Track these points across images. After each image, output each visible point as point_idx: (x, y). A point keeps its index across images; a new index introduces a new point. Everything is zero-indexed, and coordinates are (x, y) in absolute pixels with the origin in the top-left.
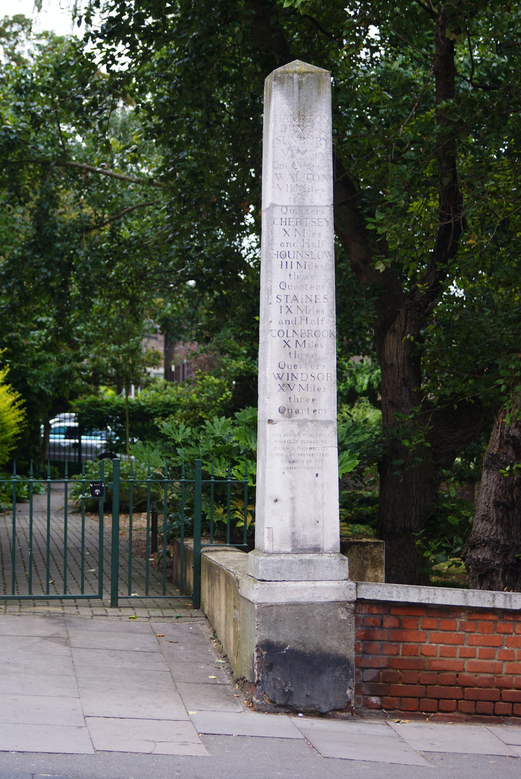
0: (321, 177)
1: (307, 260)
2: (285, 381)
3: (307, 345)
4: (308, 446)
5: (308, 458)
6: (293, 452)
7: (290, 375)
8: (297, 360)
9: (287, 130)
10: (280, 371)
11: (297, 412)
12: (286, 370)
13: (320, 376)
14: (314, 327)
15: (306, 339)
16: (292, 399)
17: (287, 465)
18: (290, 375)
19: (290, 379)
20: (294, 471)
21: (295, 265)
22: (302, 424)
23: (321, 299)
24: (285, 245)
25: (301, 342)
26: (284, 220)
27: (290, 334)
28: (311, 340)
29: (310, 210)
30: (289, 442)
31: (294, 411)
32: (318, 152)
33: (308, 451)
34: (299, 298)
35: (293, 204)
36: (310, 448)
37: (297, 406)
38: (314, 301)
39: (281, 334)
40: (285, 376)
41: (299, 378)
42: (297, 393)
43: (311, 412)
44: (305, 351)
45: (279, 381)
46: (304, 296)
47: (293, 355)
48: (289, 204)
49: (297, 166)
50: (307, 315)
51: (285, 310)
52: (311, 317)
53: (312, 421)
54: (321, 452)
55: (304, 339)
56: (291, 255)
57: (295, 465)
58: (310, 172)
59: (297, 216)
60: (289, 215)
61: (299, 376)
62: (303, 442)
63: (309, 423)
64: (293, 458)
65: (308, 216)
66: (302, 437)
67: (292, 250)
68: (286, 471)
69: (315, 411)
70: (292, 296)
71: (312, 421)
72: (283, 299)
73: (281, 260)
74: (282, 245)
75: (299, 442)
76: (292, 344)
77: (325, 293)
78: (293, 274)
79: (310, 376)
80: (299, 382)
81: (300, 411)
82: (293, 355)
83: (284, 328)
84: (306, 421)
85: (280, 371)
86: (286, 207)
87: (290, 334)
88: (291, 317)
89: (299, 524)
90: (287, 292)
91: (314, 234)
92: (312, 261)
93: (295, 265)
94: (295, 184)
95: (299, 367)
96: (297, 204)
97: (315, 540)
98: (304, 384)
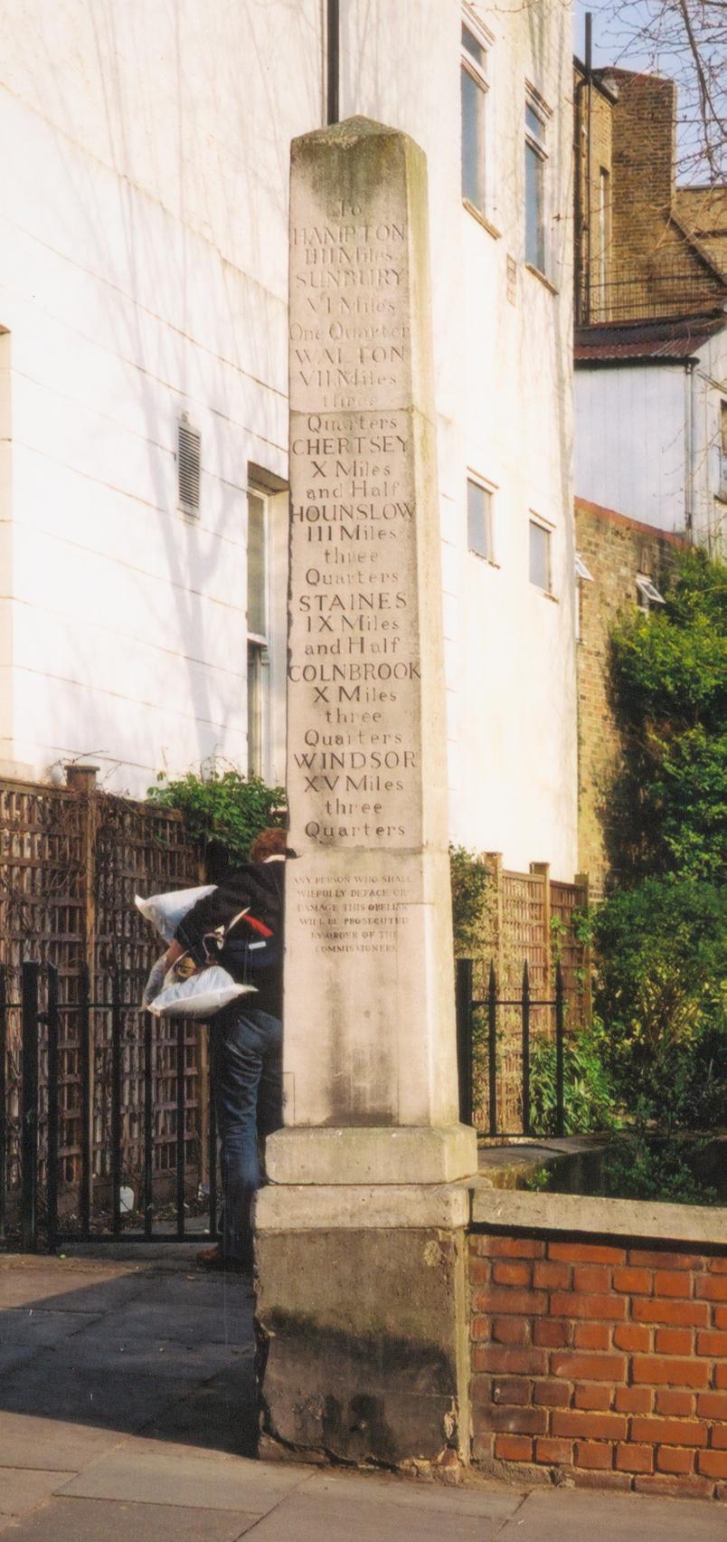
4: (367, 901)
6: (334, 915)
7: (328, 758)
10: (308, 750)
12: (320, 748)
13: (392, 759)
14: (378, 659)
15: (361, 682)
17: (321, 942)
18: (328, 758)
20: (336, 954)
24: (317, 494)
26: (313, 444)
27: (328, 673)
30: (327, 894)
31: (336, 831)
33: (365, 914)
34: (346, 601)
35: (331, 408)
36: (371, 908)
37: (343, 821)
39: (310, 674)
40: (318, 760)
42: (341, 793)
43: (372, 833)
45: (305, 771)
47: (334, 718)
51: (317, 624)
52: (371, 637)
56: (329, 515)
57: (340, 943)
64: (336, 928)
65: (360, 433)
67: (329, 502)
72: (314, 603)
74: (310, 493)
76: (332, 694)
79: (369, 759)
80: (346, 771)
82: (334, 718)
84: (360, 850)
85: (308, 750)
86: (318, 416)
87: (328, 673)
88: (328, 639)
89: (349, 1067)
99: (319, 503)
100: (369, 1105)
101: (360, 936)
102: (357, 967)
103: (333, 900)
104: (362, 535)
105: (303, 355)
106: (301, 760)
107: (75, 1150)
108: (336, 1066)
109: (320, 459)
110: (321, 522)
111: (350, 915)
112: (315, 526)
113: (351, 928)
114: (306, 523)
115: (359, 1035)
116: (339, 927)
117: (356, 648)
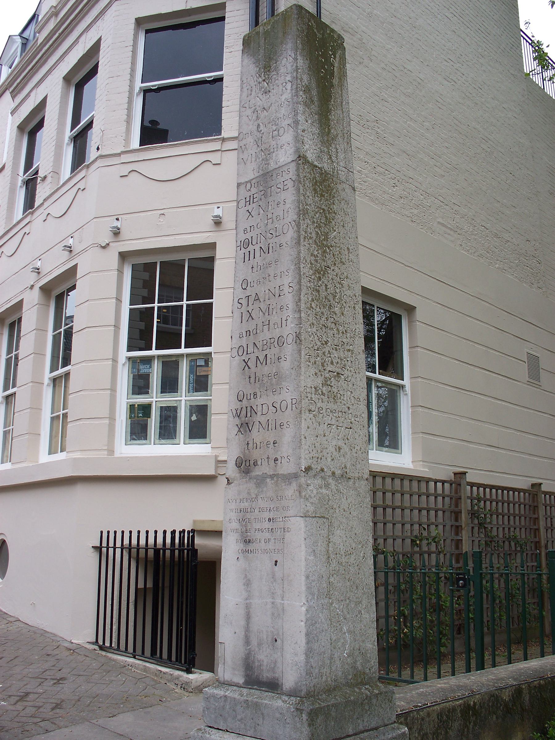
1: (270, 241)
2: (243, 419)
3: (268, 361)
4: (267, 515)
5: (267, 535)
7: (249, 409)
8: (257, 385)
14: (277, 333)
16: (251, 445)
17: (242, 546)
18: (249, 409)
19: (249, 415)
20: (250, 555)
22: (260, 481)
23: (286, 289)
25: (262, 358)
26: (248, 199)
28: (272, 353)
29: (274, 175)
30: (245, 511)
31: (252, 462)
32: (283, 100)
33: (267, 525)
36: (269, 520)
38: (277, 295)
41: (259, 413)
42: (257, 435)
43: (272, 462)
44: (266, 370)
46: (267, 291)
47: (252, 379)
49: (262, 127)
50: (269, 318)
52: (275, 318)
53: (272, 477)
55: (265, 353)
57: (250, 547)
58: (274, 128)
60: (254, 190)
62: (261, 510)
63: (268, 480)
66: (261, 503)
68: (241, 556)
69: (276, 460)
70: (254, 295)
71: (272, 477)
72: (244, 302)
75: (257, 511)
78: (255, 266)
79: (271, 408)
80: (259, 418)
81: (259, 463)
82: (252, 379)
83: (244, 343)
85: (238, 405)
86: (250, 181)
88: (251, 326)
89: (254, 642)
92: (276, 240)
94: (259, 149)
95: (259, 394)
96: (261, 172)
97: (273, 670)
98: (263, 420)
100: (266, 675)
101: (263, 542)
102: (263, 563)
103: (248, 516)
106: (235, 412)
107: (401, 608)
108: (247, 641)
109: (250, 208)
110: (251, 248)
111: (257, 526)
113: (259, 535)
115: (262, 621)
116: (252, 535)
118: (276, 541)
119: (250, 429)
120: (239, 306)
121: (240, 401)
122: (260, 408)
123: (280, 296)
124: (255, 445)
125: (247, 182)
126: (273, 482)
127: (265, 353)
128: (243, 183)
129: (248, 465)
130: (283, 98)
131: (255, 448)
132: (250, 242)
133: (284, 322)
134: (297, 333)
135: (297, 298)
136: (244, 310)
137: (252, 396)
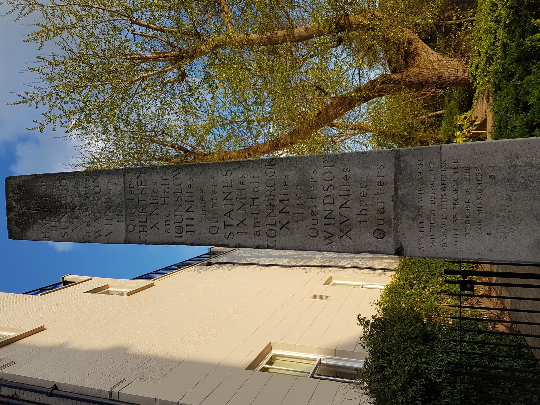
0: (95, 184)
4: (439, 192)
7: (327, 221)
9: (56, 224)
10: (322, 235)
11: (382, 211)
13: (328, 176)
18: (327, 221)
19: (332, 221)
21: (191, 215)
23: (227, 179)
24: (168, 227)
25: (281, 206)
27: (270, 220)
29: (130, 196)
32: (72, 188)
34: (227, 208)
35: (123, 218)
36: (444, 189)
37: (372, 211)
39: (272, 233)
40: (329, 229)
41: (332, 207)
42: (353, 212)
46: (225, 202)
48: (124, 224)
51: (242, 229)
54: (449, 172)
55: (277, 202)
59: (137, 212)
60: (136, 222)
61: (327, 207)
65: (136, 199)
72: (229, 230)
73: (185, 232)
75: (433, 207)
77: (220, 175)
80: (336, 208)
81: (381, 206)
85: (322, 235)
86: (127, 226)
90: (221, 225)
91: (155, 191)
92: (184, 192)
93: (191, 215)
95: (314, 209)
99: (173, 226)
104: (191, 199)
105: (97, 235)
106: (328, 241)
110: (183, 224)
112: (186, 229)
114: (184, 234)
117: (256, 202)
118: (468, 178)
119: (346, 219)
120: (231, 236)
121: (317, 233)
122: (327, 207)
123: (231, 186)
124: (363, 212)
125: (127, 230)
126: (402, 186)
127: (277, 202)
128: (126, 235)
129: (382, 222)
130: (71, 188)
131: (366, 213)
132: (178, 224)
133: (254, 181)
134: (266, 163)
135: (237, 166)
136: (235, 231)
137: (315, 217)
